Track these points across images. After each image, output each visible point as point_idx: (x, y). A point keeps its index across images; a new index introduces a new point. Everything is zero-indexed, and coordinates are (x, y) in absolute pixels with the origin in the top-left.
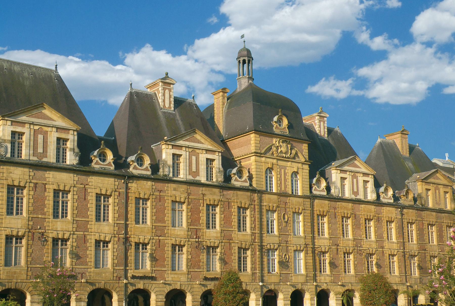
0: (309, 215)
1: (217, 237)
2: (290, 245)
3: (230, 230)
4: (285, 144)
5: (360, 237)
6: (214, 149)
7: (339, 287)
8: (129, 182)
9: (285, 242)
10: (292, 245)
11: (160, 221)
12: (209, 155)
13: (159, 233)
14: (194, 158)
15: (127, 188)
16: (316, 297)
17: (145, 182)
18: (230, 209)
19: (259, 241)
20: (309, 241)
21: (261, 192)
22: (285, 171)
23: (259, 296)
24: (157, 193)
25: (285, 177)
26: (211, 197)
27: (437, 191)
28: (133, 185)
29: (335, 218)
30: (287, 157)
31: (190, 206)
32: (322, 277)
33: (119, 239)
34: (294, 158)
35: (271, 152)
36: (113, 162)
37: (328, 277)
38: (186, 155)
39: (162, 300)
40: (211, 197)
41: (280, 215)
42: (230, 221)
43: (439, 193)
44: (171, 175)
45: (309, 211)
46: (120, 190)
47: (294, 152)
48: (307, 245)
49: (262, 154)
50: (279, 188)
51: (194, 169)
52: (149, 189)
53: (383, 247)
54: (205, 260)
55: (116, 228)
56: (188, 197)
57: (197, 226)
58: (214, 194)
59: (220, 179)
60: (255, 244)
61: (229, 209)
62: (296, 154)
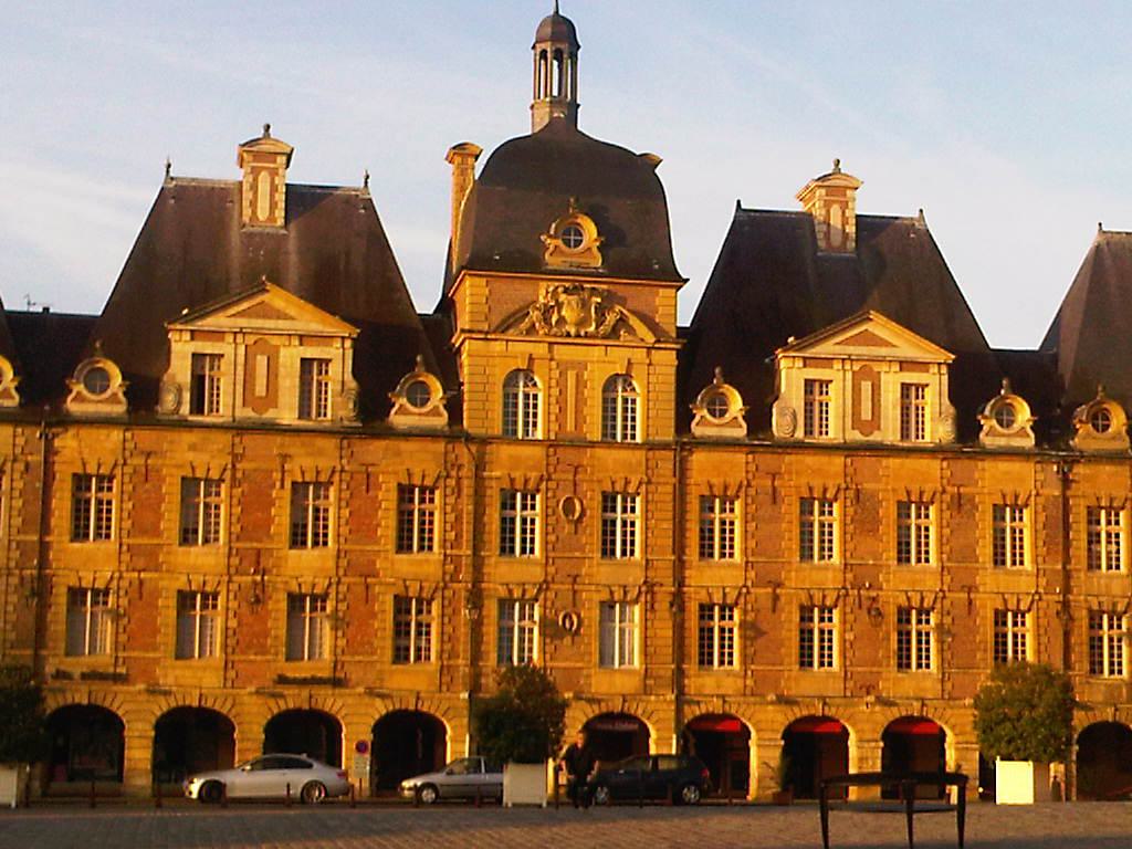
2: (587, 587)
4: (574, 299)
6: (328, 330)
7: (770, 707)
8: (55, 436)
9: (570, 580)
10: (593, 588)
11: (144, 532)
13: (141, 563)
14: (262, 361)
15: (50, 452)
16: (674, 736)
17: (102, 433)
18: (371, 493)
21: (485, 441)
22: (578, 378)
23: (466, 729)
24: (139, 461)
26: (308, 463)
28: (67, 442)
29: (774, 502)
30: (582, 333)
31: (240, 490)
33: (22, 578)
35: (524, 325)
36: (17, 389)
37: (731, 680)
38: (236, 355)
39: (143, 734)
41: (552, 503)
44: (185, 409)
45: (670, 489)
46: (29, 458)
47: (611, 318)
49: (487, 333)
50: (554, 427)
51: (260, 390)
52: (113, 452)
53: (970, 589)
54: (283, 632)
55: (16, 554)
56: (234, 466)
57: (260, 541)
58: (321, 453)
59: (342, 413)
60: (455, 585)
61: (368, 491)
62: (622, 320)
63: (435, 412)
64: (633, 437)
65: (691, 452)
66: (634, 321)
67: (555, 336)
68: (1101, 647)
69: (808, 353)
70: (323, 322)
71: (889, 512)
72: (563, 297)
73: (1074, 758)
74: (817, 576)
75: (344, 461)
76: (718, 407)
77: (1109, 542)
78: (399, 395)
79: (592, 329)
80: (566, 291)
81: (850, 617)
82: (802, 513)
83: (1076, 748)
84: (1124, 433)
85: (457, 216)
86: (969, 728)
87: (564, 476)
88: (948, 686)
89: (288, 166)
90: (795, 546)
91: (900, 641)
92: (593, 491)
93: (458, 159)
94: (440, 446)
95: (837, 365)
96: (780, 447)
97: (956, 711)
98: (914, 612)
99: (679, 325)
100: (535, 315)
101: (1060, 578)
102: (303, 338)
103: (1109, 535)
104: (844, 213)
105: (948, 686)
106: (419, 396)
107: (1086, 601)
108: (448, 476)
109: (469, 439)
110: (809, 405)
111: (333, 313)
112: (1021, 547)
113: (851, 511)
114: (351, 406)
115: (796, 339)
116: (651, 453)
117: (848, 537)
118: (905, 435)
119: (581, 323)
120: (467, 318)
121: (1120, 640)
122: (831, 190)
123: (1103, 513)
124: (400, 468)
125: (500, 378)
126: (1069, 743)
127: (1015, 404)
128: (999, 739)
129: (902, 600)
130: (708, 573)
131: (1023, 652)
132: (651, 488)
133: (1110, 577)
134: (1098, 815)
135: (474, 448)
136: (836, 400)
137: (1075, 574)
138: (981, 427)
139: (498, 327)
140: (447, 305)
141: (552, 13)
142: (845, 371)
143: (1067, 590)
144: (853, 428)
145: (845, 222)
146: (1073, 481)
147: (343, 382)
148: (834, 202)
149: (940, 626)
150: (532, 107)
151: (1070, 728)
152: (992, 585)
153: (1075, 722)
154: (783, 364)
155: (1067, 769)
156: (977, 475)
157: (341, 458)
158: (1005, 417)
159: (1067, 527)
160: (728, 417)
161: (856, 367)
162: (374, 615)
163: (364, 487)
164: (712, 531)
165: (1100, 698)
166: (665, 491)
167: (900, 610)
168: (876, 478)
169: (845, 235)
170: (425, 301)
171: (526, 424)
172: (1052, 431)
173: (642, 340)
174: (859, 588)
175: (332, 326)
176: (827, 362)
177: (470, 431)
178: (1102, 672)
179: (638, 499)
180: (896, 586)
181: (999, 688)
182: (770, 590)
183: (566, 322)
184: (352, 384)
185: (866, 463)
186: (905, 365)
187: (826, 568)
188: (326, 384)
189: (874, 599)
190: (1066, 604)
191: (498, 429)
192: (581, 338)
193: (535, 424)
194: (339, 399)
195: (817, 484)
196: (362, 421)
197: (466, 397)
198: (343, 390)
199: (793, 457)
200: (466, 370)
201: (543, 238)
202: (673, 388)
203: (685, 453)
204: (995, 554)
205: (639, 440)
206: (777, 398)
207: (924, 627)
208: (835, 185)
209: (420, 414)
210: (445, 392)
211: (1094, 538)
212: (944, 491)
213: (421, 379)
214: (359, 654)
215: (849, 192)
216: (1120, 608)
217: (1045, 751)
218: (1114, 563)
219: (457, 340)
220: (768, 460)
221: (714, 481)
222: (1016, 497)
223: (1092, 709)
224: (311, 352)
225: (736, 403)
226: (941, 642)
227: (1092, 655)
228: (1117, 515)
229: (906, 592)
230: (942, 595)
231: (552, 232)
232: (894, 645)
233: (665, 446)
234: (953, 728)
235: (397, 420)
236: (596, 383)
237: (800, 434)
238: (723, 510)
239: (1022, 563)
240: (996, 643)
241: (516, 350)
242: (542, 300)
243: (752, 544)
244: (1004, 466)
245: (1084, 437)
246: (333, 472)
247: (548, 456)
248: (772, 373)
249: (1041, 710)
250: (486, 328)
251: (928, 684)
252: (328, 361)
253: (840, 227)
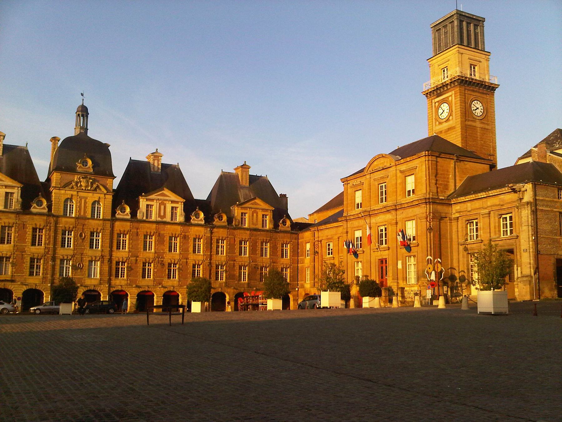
1: (10, 250)
4: (85, 180)
5: (163, 250)
6: (14, 185)
7: (134, 288)
9: (81, 254)
10: (87, 257)
12: (8, 189)
18: (25, 230)
19: (52, 253)
20: (107, 253)
21: (58, 217)
22: (85, 201)
26: (6, 221)
27: (255, 215)
30: (87, 189)
34: (95, 190)
35: (70, 186)
40: (6, 221)
41: (76, 234)
43: (257, 216)
45: (109, 231)
47: (95, 186)
49: (60, 188)
50: (78, 214)
53: (187, 259)
58: (10, 218)
59: (17, 207)
60: (48, 255)
62: (98, 187)
63: (44, 208)
64: (100, 217)
65: (115, 222)
66: (101, 187)
67: (79, 190)
68: (218, 274)
69: (147, 198)
70: (12, 182)
71: (167, 239)
72: (81, 180)
73: (211, 301)
74: (148, 255)
75: (17, 221)
76: (123, 210)
77: (221, 248)
78: (34, 204)
79: (89, 188)
80: (83, 178)
81: (156, 265)
82: (144, 238)
83: (211, 298)
84: (226, 221)
85: (52, 156)
86: (185, 294)
87: (80, 227)
88: (180, 283)
89: (4, 139)
90: (142, 247)
91: (168, 272)
92: (88, 231)
93: (53, 141)
94: (45, 218)
95: (155, 201)
96: (139, 221)
97: (182, 289)
98: (172, 264)
99: (113, 188)
100: (74, 184)
101: (209, 256)
102: (6, 187)
103: (221, 246)
104: (158, 162)
105: (180, 283)
106: (40, 204)
107: (215, 262)
108: (47, 226)
109: (54, 216)
110: (147, 211)
111: (16, 180)
112: (200, 249)
113: (157, 238)
114: (20, 205)
115: (145, 194)
116: (104, 222)
117: (156, 245)
118: (172, 220)
119: (86, 187)
120: (54, 183)
121: (223, 272)
122: (155, 157)
123: (220, 241)
124: (33, 223)
125: (63, 200)
126: (210, 297)
127: (200, 213)
128: (192, 296)
129: (169, 261)
130: (118, 253)
131: (200, 275)
132: (104, 231)
133: (222, 256)
134: (217, 315)
135: (55, 218)
136: (154, 210)
137: (213, 255)
138: (191, 218)
139: (63, 186)
140: (49, 180)
141: (81, 104)
142: (157, 203)
143: (211, 259)
144: (159, 217)
145: (158, 165)
146: (213, 233)
147: (18, 199)
148: (156, 159)
149: (179, 268)
150: (75, 129)
151: (211, 294)
152: (192, 258)
153: (211, 292)
154: (141, 200)
155: (209, 305)
156: (190, 230)
157: (16, 220)
158: (197, 216)
159: (211, 244)
160: (126, 213)
161: (160, 202)
162: (24, 263)
163: (22, 228)
164: (120, 242)
165: (218, 286)
166: (108, 232)
167: (169, 264)
168: (164, 230)
169: (158, 168)
170: (42, 178)
171: (70, 213)
172: (209, 220)
173: (103, 192)
174: (159, 258)
175: (15, 183)
176: (152, 200)
177: (54, 214)
178: (218, 280)
179: (100, 234)
180: (168, 257)
181: (193, 284)
182: (135, 258)
183: (82, 186)
184: (20, 200)
185: (161, 226)
186: (173, 202)
187: (150, 253)
188: (13, 200)
189: (162, 261)
190: (210, 263)
191: (62, 213)
192: (86, 191)
193: (72, 213)
194: (16, 204)
195: (149, 231)
196: (23, 210)
197: (53, 205)
198: (17, 201)
199: (143, 224)
200: (53, 198)
201: (76, 163)
202: (111, 205)
203: (114, 222)
204: (194, 250)
205: (101, 218)
206: (139, 209)
207: (175, 268)
208: (156, 155)
209: (39, 209)
210: (47, 203)
211: (218, 247)
212: (181, 234)
213: (41, 199)
214: (19, 273)
215: (159, 157)
216: (223, 264)
217: (204, 299)
218: (222, 253)
219: (51, 189)
220: (136, 225)
221: (121, 229)
222: (199, 236)
223: (215, 289)
224: (8, 190)
225: (128, 210)
226: (179, 272)
227: (216, 275)
228: (224, 241)
229: (171, 259)
230: (179, 260)
231: (79, 162)
232: (167, 273)
233: (108, 220)
234: (181, 293)
235: (33, 210)
236: (90, 203)
237: (145, 218)
238: (123, 237)
239: (200, 252)
240: (193, 272)
241: (69, 193)
242: (76, 180)
243: (131, 246)
244: (196, 228)
245: (216, 222)
246: (14, 224)
247: (76, 222)
248: (138, 202)
249: (203, 289)
250: (59, 186)
251: (175, 282)
252: (13, 193)
253: (157, 166)
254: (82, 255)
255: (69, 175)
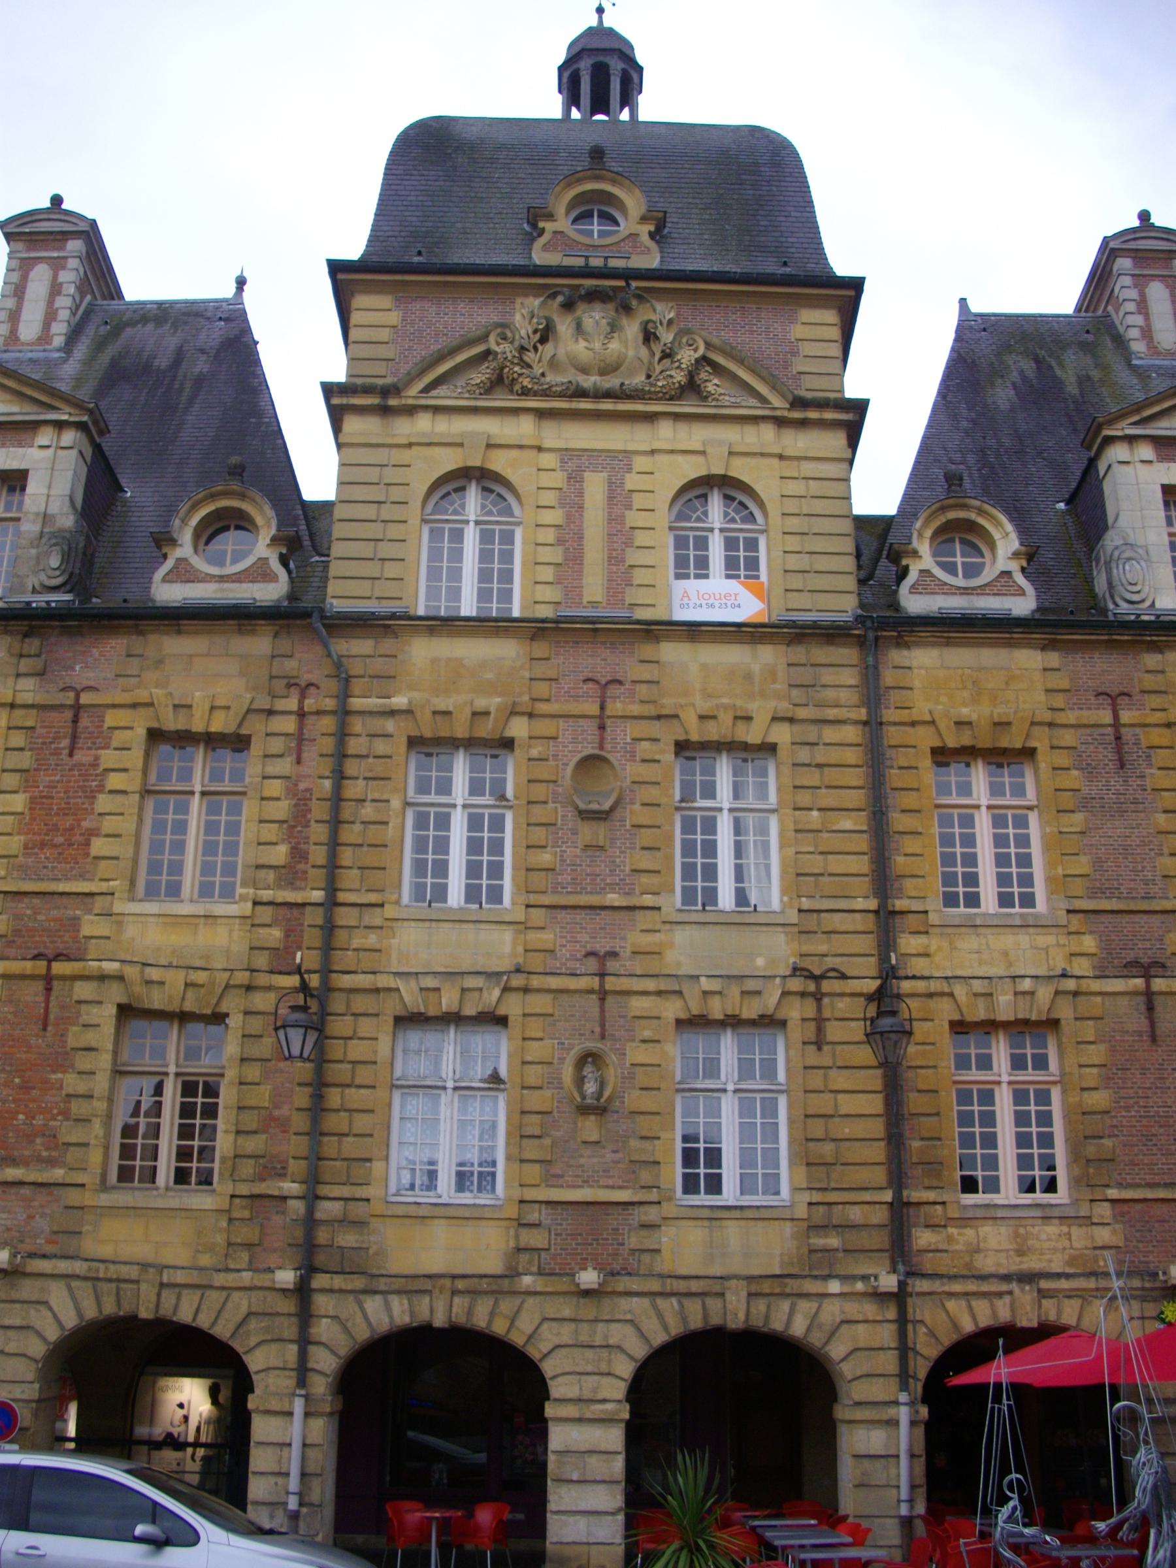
0: (851, 756)
3: (61, 887)
18: (81, 756)
25: (615, 521)
32: (987, 1230)
42: (72, 828)
48: (817, 979)
61: (71, 755)
162: (62, 1060)
163: (65, 743)
254: (602, 975)
255: (461, 306)
